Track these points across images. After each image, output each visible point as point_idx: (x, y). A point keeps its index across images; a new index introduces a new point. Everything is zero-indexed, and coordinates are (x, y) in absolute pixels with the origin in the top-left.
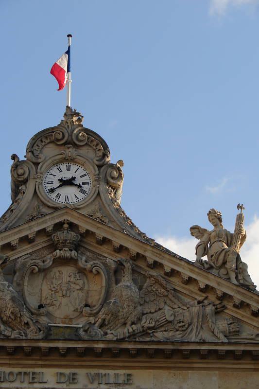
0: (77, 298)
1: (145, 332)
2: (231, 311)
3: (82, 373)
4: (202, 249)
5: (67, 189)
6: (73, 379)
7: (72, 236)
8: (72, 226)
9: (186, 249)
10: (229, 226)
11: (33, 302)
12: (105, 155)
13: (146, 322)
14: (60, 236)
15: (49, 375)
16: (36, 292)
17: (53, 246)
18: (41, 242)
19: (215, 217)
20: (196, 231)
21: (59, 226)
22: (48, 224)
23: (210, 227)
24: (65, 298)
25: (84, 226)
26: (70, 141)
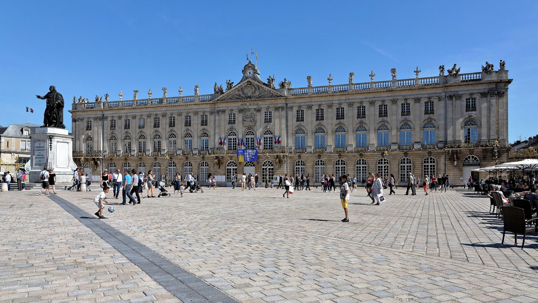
0: (251, 92)
16: (246, 91)
22: (246, 81)
24: (249, 92)
25: (251, 81)
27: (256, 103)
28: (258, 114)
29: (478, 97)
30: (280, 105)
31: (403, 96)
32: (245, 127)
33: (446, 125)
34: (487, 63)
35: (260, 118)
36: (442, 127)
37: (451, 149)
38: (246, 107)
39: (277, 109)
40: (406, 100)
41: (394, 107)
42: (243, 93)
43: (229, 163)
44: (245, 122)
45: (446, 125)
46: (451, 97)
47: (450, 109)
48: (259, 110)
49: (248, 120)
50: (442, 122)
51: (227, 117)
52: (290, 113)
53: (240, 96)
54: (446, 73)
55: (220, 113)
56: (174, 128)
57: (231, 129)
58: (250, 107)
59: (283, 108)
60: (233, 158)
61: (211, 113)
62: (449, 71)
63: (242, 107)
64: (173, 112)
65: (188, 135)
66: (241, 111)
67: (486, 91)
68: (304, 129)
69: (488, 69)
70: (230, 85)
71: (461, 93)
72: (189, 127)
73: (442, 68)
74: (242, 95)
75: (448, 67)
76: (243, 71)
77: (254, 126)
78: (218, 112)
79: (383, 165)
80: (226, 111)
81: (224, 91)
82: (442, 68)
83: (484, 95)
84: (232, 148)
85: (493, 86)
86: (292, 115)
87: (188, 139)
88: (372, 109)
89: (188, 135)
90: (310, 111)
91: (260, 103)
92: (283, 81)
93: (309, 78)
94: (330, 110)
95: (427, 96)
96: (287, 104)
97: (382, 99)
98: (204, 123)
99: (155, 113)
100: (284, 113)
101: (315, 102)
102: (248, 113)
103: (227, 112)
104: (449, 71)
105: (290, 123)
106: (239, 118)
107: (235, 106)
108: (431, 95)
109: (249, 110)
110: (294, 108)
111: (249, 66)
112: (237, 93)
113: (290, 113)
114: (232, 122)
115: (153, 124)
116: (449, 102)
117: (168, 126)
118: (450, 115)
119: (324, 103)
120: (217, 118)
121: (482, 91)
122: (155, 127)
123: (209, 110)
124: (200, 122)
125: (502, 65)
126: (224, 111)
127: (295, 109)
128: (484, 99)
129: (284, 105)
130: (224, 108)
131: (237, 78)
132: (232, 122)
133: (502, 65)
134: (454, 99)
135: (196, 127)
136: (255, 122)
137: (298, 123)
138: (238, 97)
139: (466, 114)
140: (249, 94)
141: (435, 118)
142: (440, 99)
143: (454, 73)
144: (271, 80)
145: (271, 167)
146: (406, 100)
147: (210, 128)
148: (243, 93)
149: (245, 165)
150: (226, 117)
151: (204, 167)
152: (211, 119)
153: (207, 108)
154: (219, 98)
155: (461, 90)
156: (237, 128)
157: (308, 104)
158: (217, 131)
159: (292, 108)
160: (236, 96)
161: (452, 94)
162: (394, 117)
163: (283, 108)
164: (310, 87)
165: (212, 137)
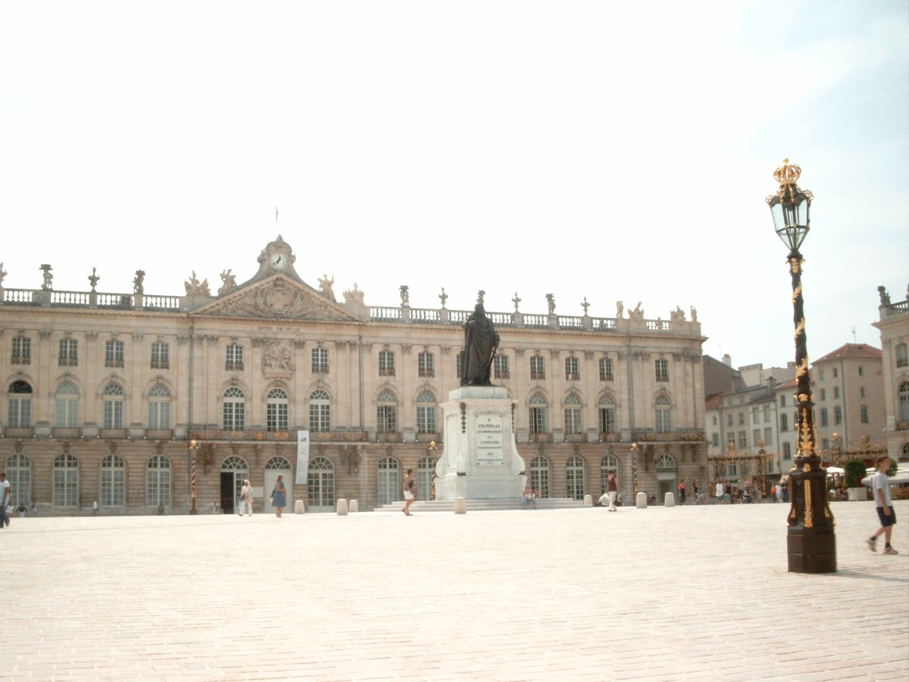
1: (303, 315)
2: (329, 308)
3: (284, 328)
4: (321, 286)
5: (278, 261)
6: (281, 329)
7: (281, 282)
8: (282, 280)
9: (316, 286)
10: (329, 279)
11: (269, 303)
12: (291, 251)
13: (304, 312)
14: (278, 282)
15: (275, 328)
16: (270, 299)
17: (275, 285)
18: (271, 284)
19: (325, 276)
20: (319, 280)
21: (277, 279)
22: (274, 277)
23: (324, 279)
24: (279, 302)
25: (286, 278)
26: (279, 246)
27: (294, 328)
28: (299, 352)
29: (669, 358)
30: (347, 338)
31: (569, 345)
32: (267, 378)
33: (631, 401)
34: (678, 307)
35: (303, 361)
36: (625, 404)
37: (645, 443)
38: (270, 335)
39: (339, 345)
40: (572, 352)
41: (555, 362)
42: (265, 303)
43: (227, 462)
44: (268, 369)
45: (631, 401)
46: (636, 355)
47: (636, 376)
48: (300, 345)
49: (273, 363)
50: (625, 396)
51: (224, 353)
52: (366, 356)
53: (256, 306)
54: (626, 316)
55: (205, 343)
56: (72, 370)
57: (234, 381)
58: (280, 336)
59: (352, 345)
60: (241, 451)
61: (180, 340)
62: (629, 311)
63: (261, 336)
64: (73, 328)
65: (114, 387)
66: (256, 342)
67: (679, 351)
68: (395, 391)
69: (677, 316)
70: (228, 279)
71: (648, 350)
72: (118, 371)
73: (620, 308)
74: (262, 307)
75: (629, 306)
76: (263, 254)
77: (289, 379)
78: (201, 339)
79: (539, 469)
80: (221, 339)
81: (214, 293)
82: (620, 308)
83: (677, 357)
84: (234, 426)
85: (687, 345)
86: (371, 360)
87: (114, 398)
88: (520, 363)
89: (114, 387)
90: (407, 357)
91: (303, 330)
92: (352, 289)
93: (404, 289)
94: (445, 357)
95: (603, 349)
96: (360, 338)
97: (536, 346)
98: (160, 360)
99: (16, 326)
100: (355, 355)
101: (418, 338)
102: (276, 350)
103: (225, 342)
104: (629, 311)
105: (367, 379)
106: (253, 357)
107: (244, 331)
108: (607, 349)
109: (278, 341)
110: (374, 346)
111: (279, 246)
112: (248, 301)
113: (366, 356)
114: (235, 364)
115: (9, 355)
116: (635, 364)
117: (56, 361)
118: (637, 384)
119: (435, 343)
120: (197, 352)
121: (675, 351)
122: (15, 360)
123: (174, 332)
124: (149, 359)
125: (694, 313)
126: (214, 339)
127: (377, 349)
128: (678, 364)
129: (357, 339)
130: (216, 333)
131: (246, 271)
132: (235, 364)
133: (694, 313)
134: (640, 358)
135: (137, 371)
136: (293, 370)
137: (385, 378)
138: (253, 310)
139: (657, 386)
140: (278, 306)
141: (615, 389)
142: (620, 356)
143: (637, 315)
144: (327, 285)
145: (328, 472)
146: (572, 352)
147: (177, 377)
148: (265, 303)
149: (268, 467)
150: (218, 354)
151: (113, 469)
152: (178, 354)
153: (171, 327)
154: (207, 307)
155: (650, 346)
156: (247, 381)
157: (404, 341)
158: (196, 383)
159: (370, 346)
160: (248, 308)
161: (638, 350)
162: (556, 382)
163: (352, 345)
164: (405, 308)
165: (183, 399)
